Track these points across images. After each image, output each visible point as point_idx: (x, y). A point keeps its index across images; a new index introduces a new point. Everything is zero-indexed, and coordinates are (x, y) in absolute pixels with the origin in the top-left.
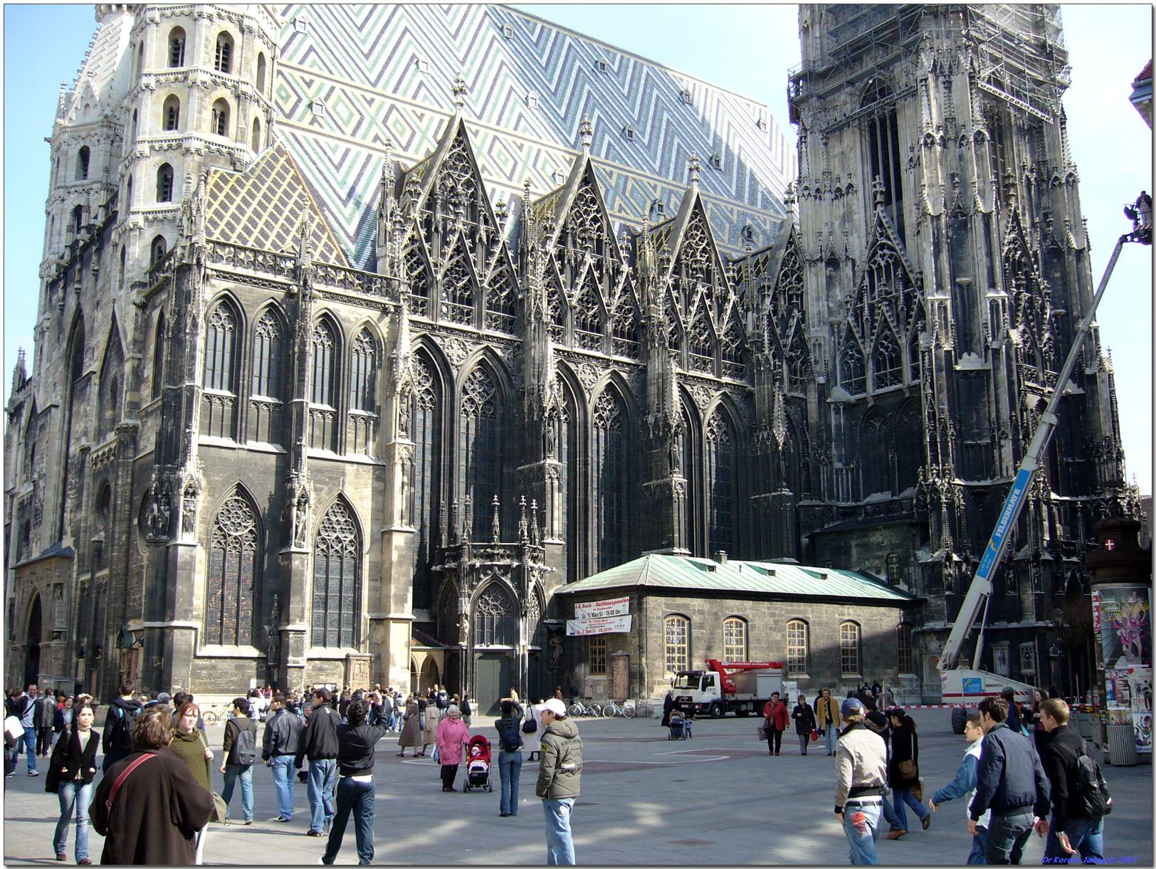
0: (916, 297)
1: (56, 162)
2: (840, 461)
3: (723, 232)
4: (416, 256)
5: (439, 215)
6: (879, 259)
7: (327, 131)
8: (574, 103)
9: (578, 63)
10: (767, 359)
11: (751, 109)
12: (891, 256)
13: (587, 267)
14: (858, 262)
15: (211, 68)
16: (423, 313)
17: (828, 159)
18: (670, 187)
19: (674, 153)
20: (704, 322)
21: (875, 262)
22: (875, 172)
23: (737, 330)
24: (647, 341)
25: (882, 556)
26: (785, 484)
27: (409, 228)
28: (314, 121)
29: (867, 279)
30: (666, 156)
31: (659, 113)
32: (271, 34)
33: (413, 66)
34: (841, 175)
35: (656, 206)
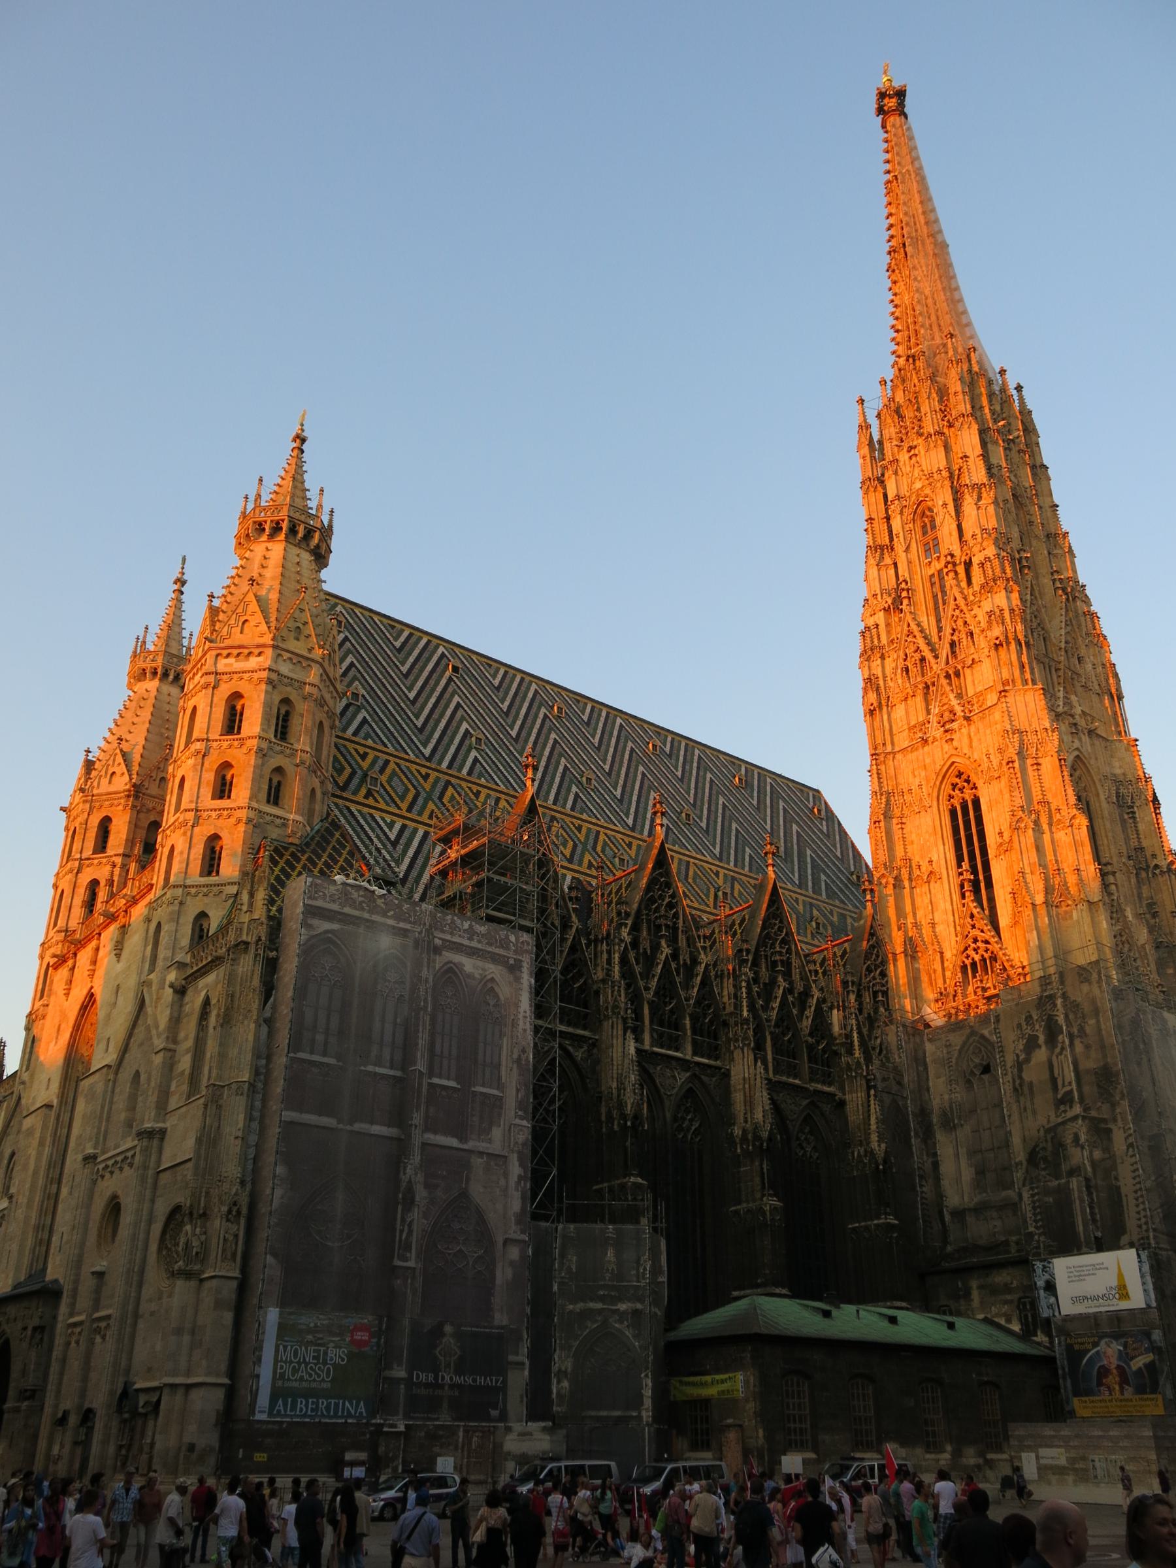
1: (72, 835)
6: (973, 953)
7: (383, 806)
8: (629, 785)
9: (630, 744)
10: (858, 1063)
13: (663, 957)
14: (948, 955)
15: (272, 736)
19: (733, 838)
20: (785, 1020)
21: (968, 957)
22: (959, 860)
24: (729, 1040)
25: (1011, 1302)
28: (369, 794)
30: (726, 840)
31: (714, 797)
32: (331, 702)
33: (467, 742)
35: (720, 894)
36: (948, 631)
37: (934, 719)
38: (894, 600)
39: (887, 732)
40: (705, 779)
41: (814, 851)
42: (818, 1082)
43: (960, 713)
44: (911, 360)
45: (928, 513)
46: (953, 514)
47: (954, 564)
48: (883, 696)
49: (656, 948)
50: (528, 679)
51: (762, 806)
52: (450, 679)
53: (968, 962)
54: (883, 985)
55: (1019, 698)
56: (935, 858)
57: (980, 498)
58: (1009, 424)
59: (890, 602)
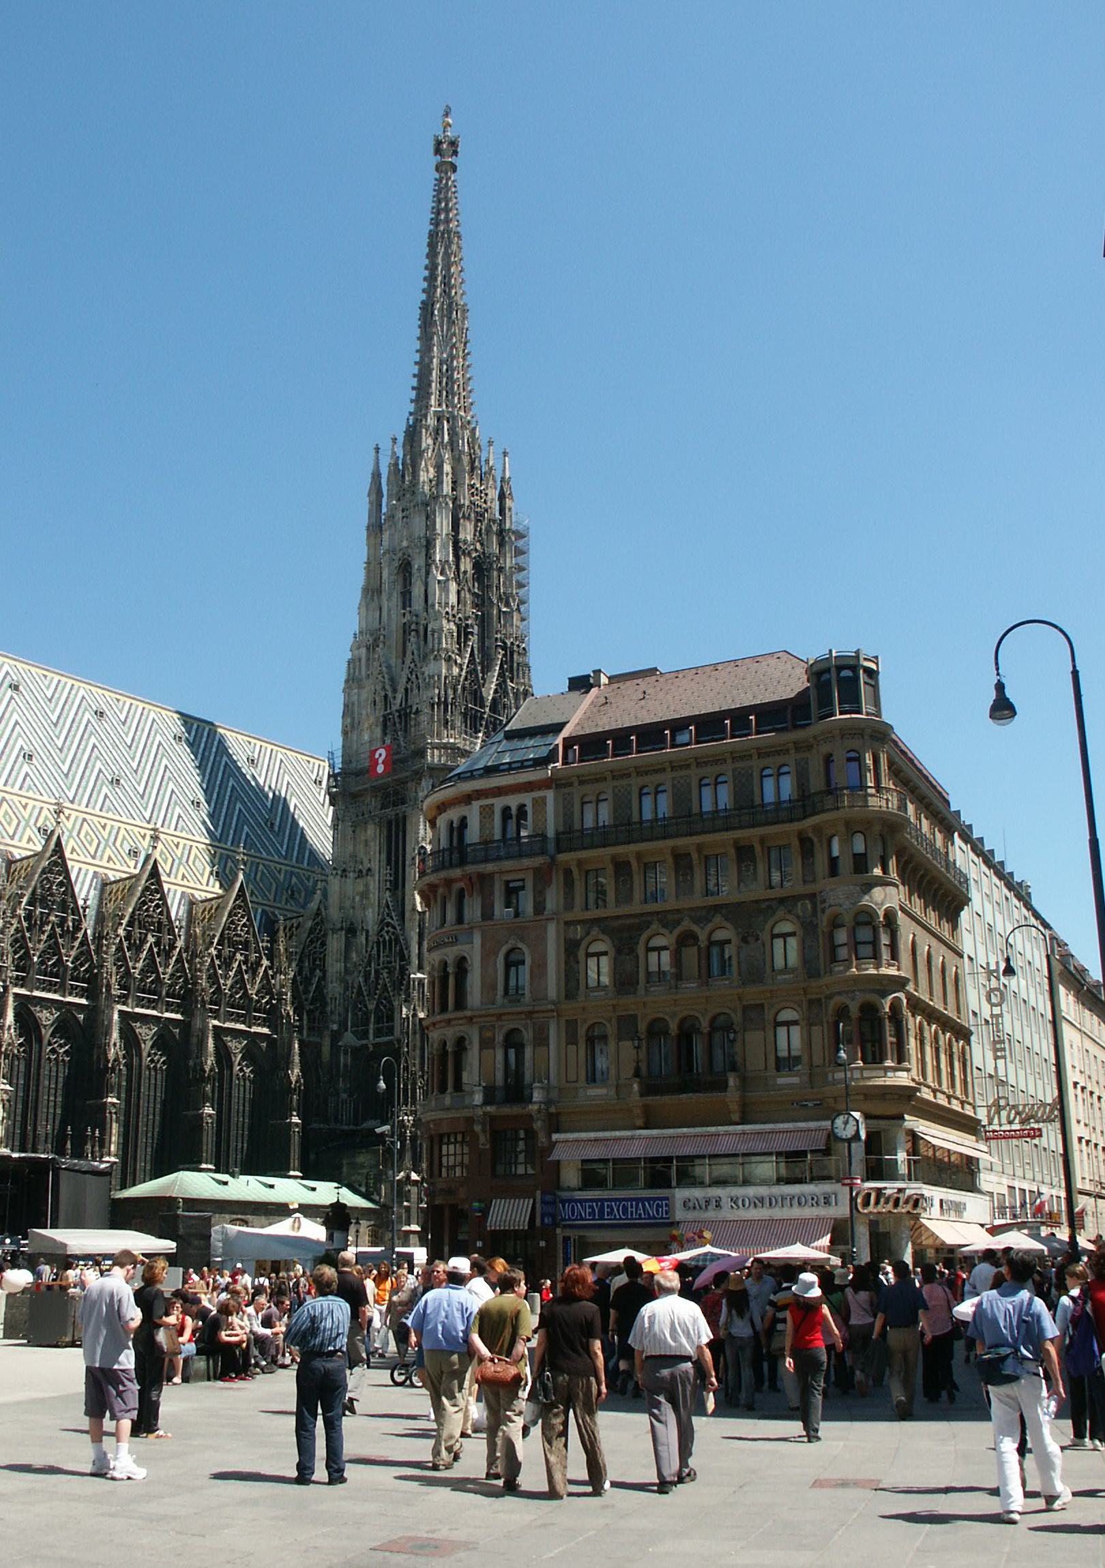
2: (345, 1092)
3: (269, 891)
4: (19, 942)
5: (39, 910)
6: (384, 933)
11: (311, 765)
12: (393, 933)
13: (148, 945)
16: (22, 986)
17: (355, 846)
18: (226, 852)
19: (235, 818)
21: (382, 936)
22: (389, 863)
23: (266, 988)
26: (295, 1113)
27: (14, 921)
29: (375, 948)
38: (375, 640)
40: (220, 762)
42: (259, 1025)
47: (417, 624)
48: (356, 721)
49: (143, 941)
50: (77, 684)
52: (12, 698)
53: (381, 940)
54: (321, 953)
57: (442, 574)
58: (486, 495)
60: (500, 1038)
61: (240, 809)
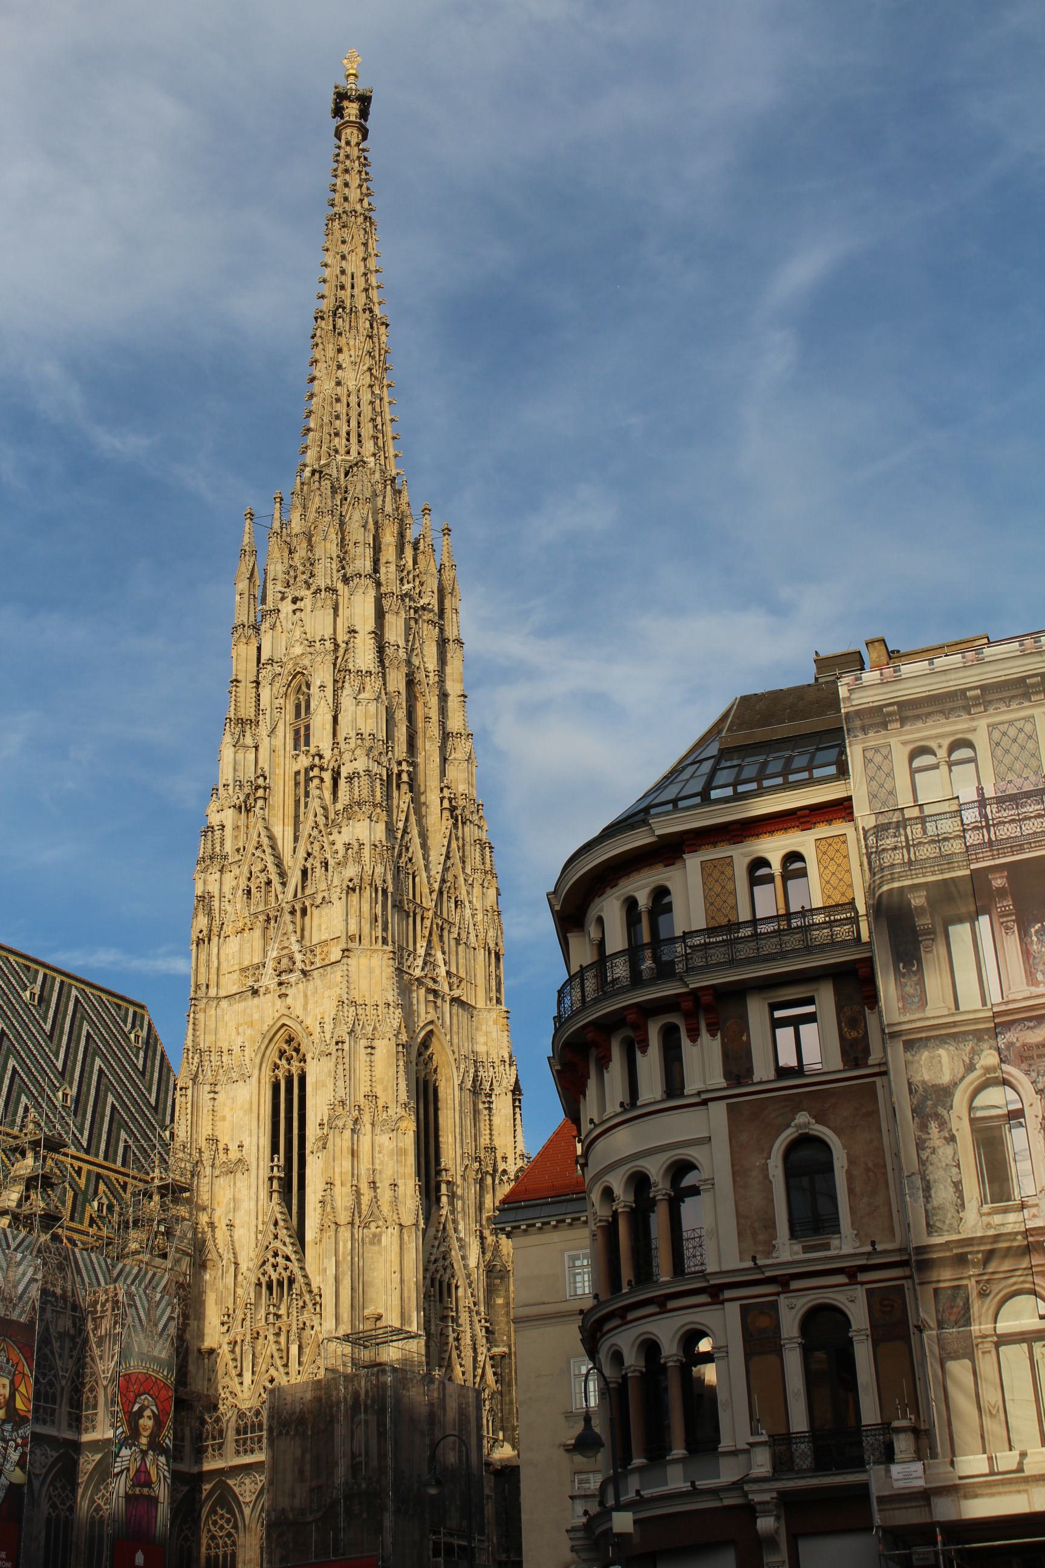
0: (313, 1327)
11: (123, 1012)
12: (286, 1269)
14: (243, 1267)
22: (275, 1149)
29: (252, 1295)
34: (230, 1147)
36: (301, 854)
37: (270, 965)
38: (248, 795)
39: (213, 971)
41: (118, 1097)
43: (299, 965)
44: (317, 475)
45: (304, 689)
46: (330, 701)
48: (216, 923)
51: (57, 1033)
53: (264, 1280)
55: (364, 961)
56: (246, 1143)
57: (362, 689)
58: (422, 584)
59: (242, 799)
60: (790, 1325)
61: (14, 1068)
